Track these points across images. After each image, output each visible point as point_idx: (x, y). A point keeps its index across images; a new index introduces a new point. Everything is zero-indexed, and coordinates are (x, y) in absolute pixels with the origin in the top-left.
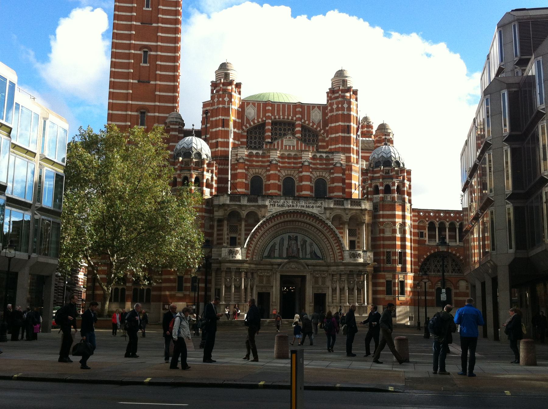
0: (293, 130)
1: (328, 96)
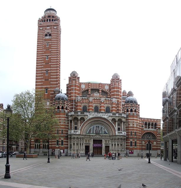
0: (99, 92)
1: (111, 81)
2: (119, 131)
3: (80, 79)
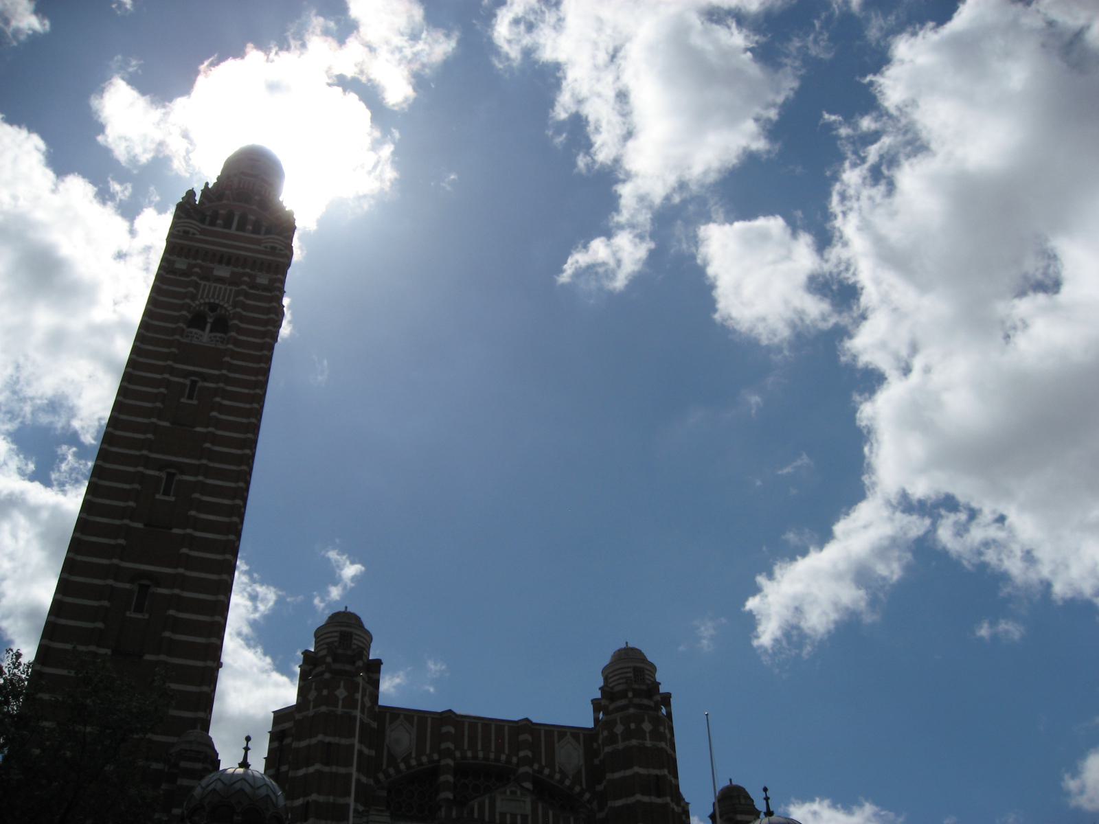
1: (597, 706)
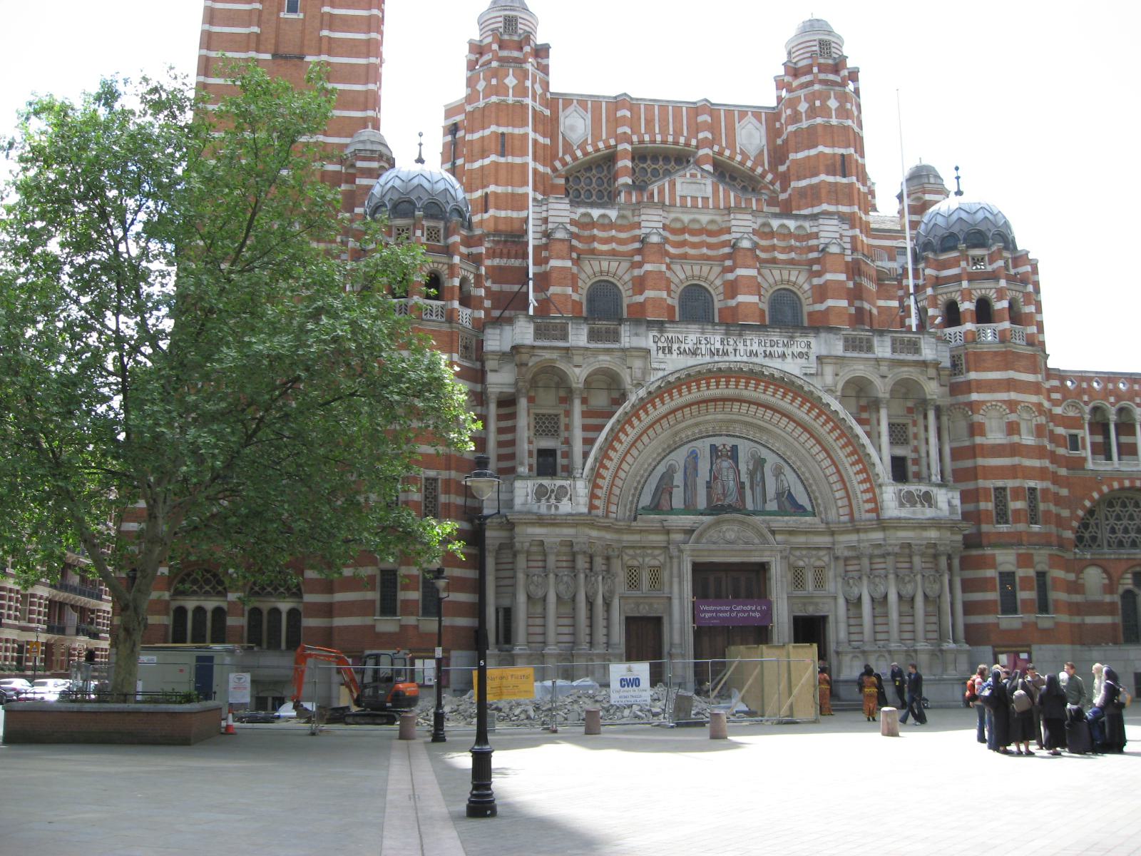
1: (780, 84)
2: (906, 488)
3: (554, 61)
